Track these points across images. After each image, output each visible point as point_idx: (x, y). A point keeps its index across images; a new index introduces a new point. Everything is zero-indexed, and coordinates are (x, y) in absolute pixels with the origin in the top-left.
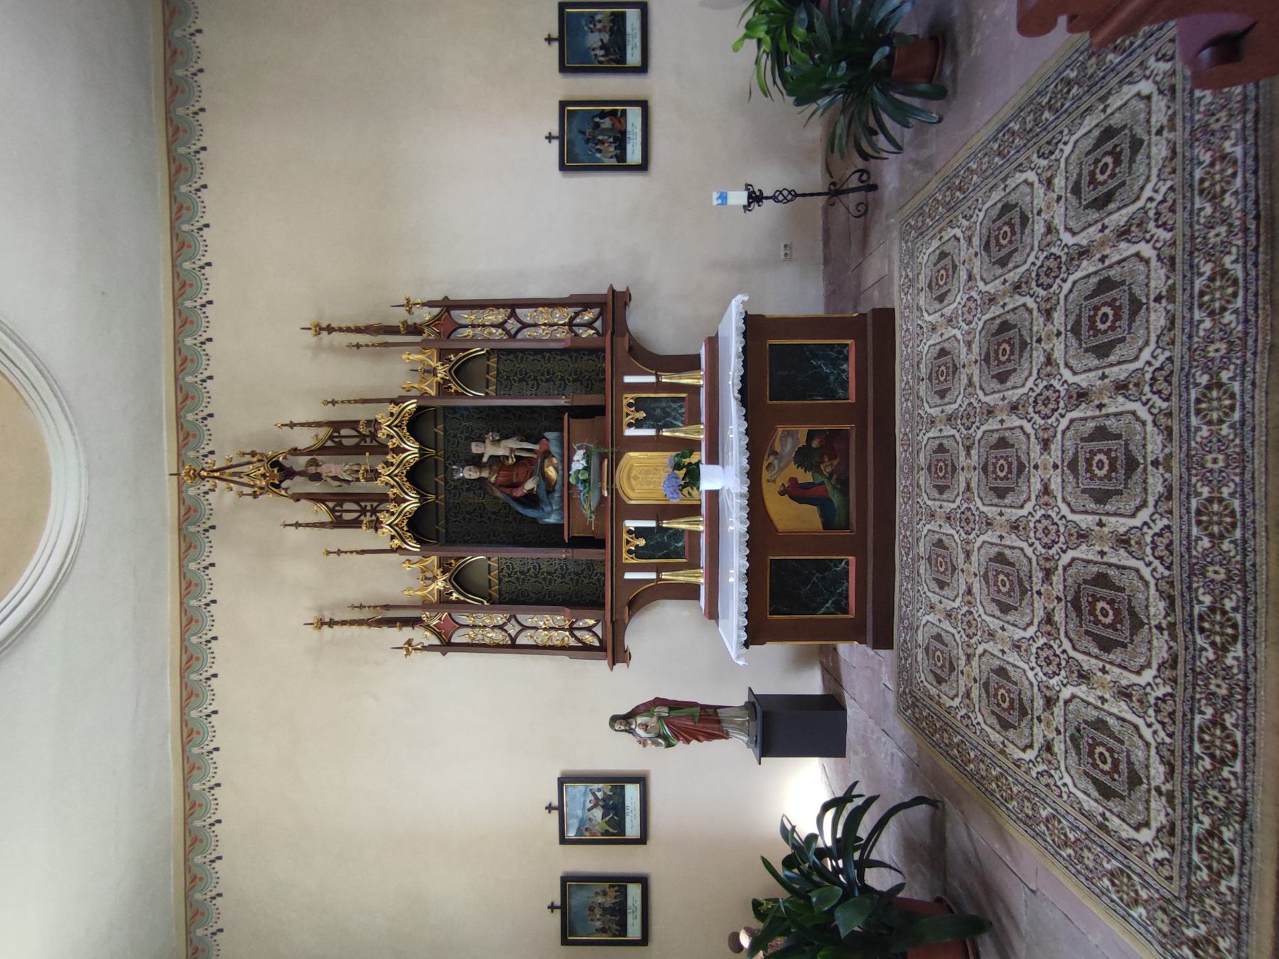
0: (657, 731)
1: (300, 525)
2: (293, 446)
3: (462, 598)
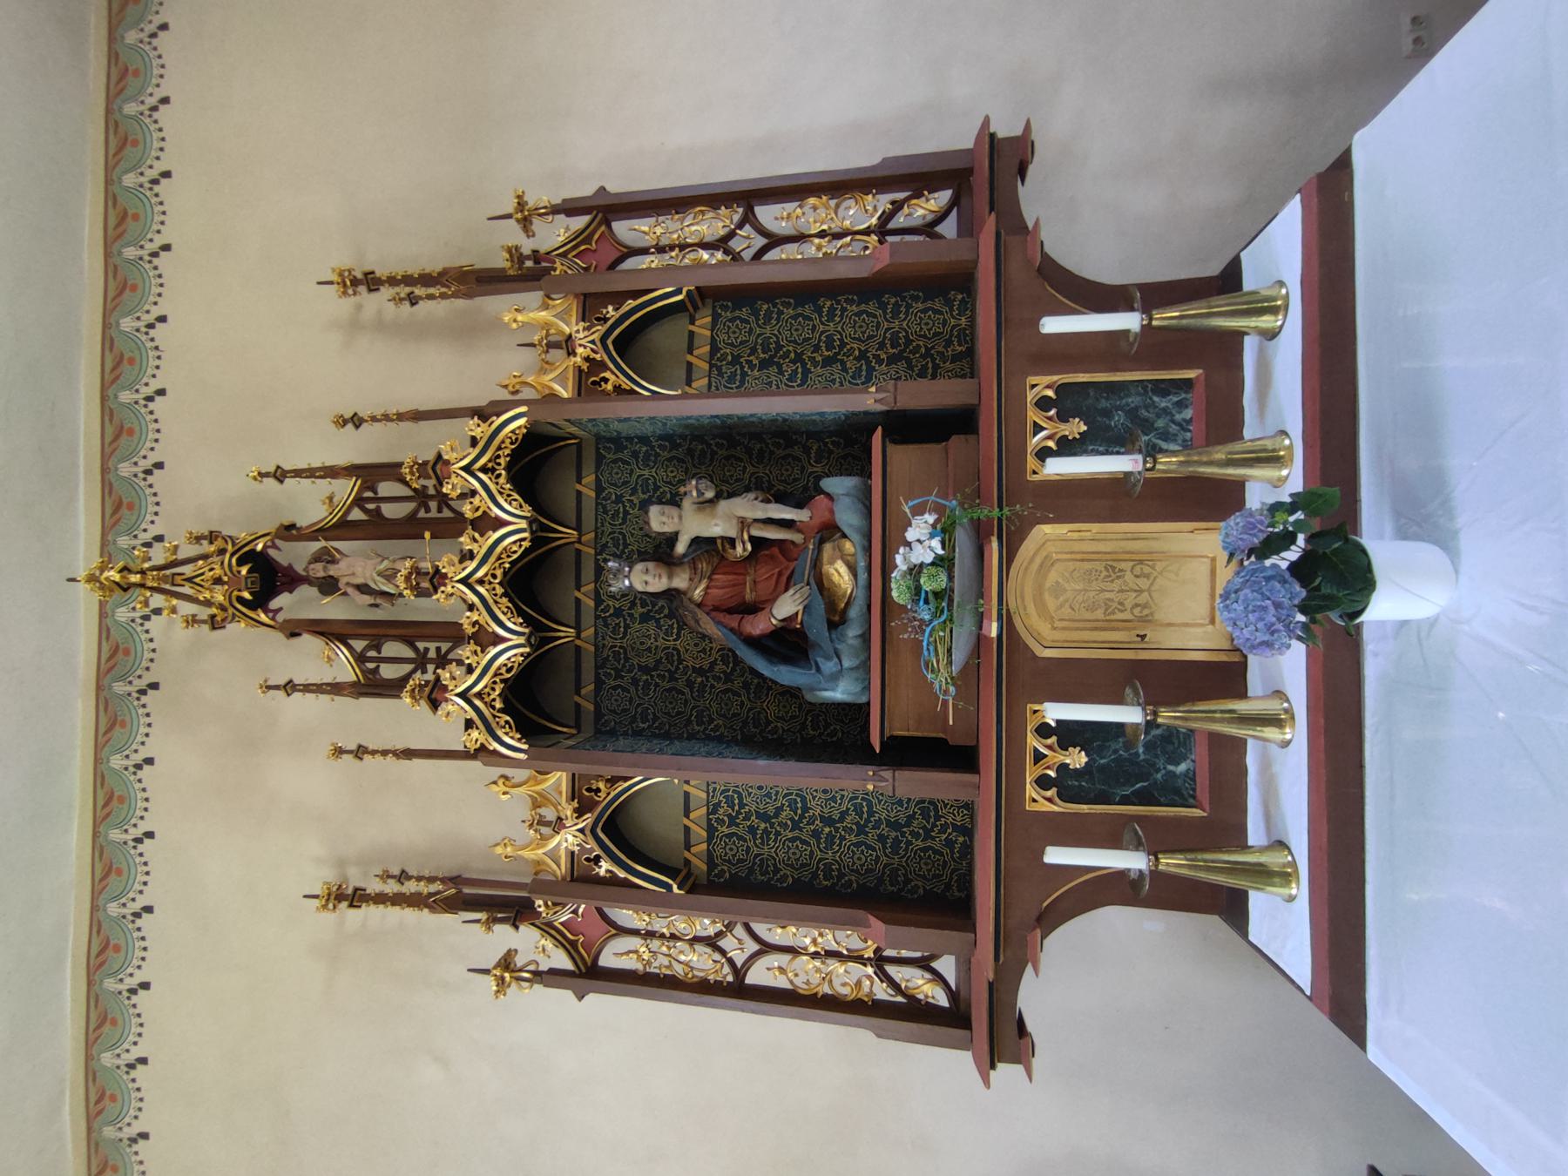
3: (622, 874)
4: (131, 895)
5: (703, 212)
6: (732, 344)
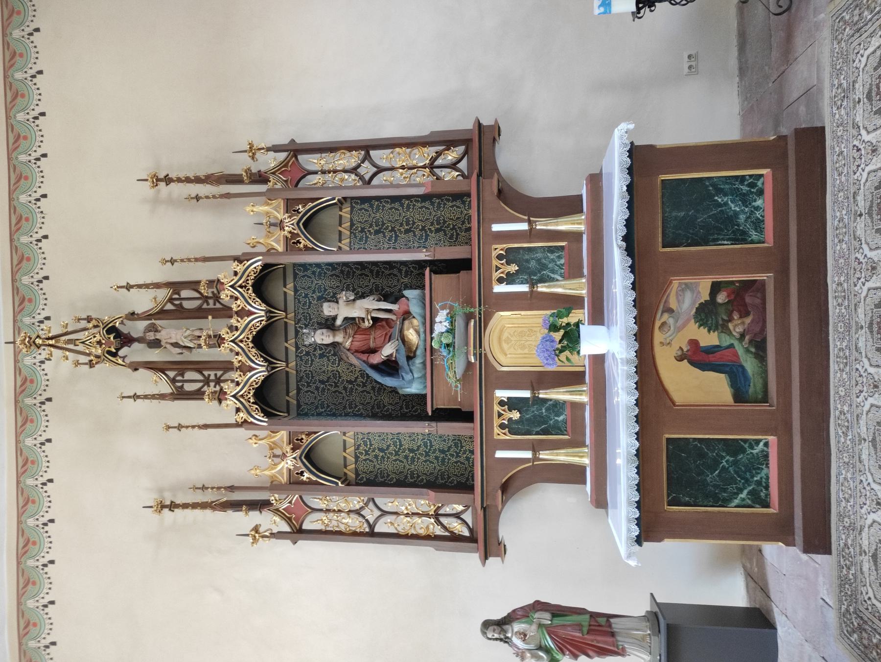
0: (538, 642)
1: (139, 397)
2: (131, 311)
3: (314, 478)
4: (41, 514)
5: (344, 154)
6: (360, 222)
